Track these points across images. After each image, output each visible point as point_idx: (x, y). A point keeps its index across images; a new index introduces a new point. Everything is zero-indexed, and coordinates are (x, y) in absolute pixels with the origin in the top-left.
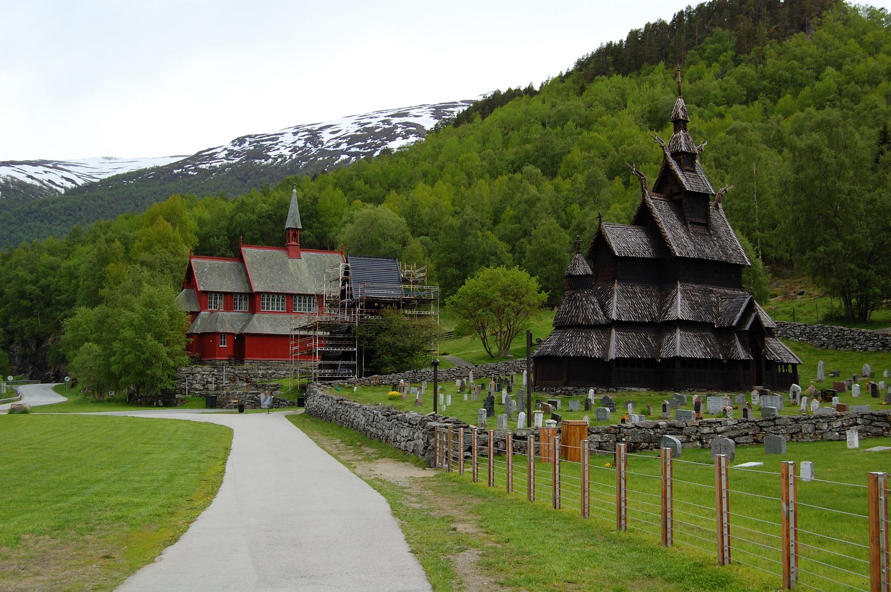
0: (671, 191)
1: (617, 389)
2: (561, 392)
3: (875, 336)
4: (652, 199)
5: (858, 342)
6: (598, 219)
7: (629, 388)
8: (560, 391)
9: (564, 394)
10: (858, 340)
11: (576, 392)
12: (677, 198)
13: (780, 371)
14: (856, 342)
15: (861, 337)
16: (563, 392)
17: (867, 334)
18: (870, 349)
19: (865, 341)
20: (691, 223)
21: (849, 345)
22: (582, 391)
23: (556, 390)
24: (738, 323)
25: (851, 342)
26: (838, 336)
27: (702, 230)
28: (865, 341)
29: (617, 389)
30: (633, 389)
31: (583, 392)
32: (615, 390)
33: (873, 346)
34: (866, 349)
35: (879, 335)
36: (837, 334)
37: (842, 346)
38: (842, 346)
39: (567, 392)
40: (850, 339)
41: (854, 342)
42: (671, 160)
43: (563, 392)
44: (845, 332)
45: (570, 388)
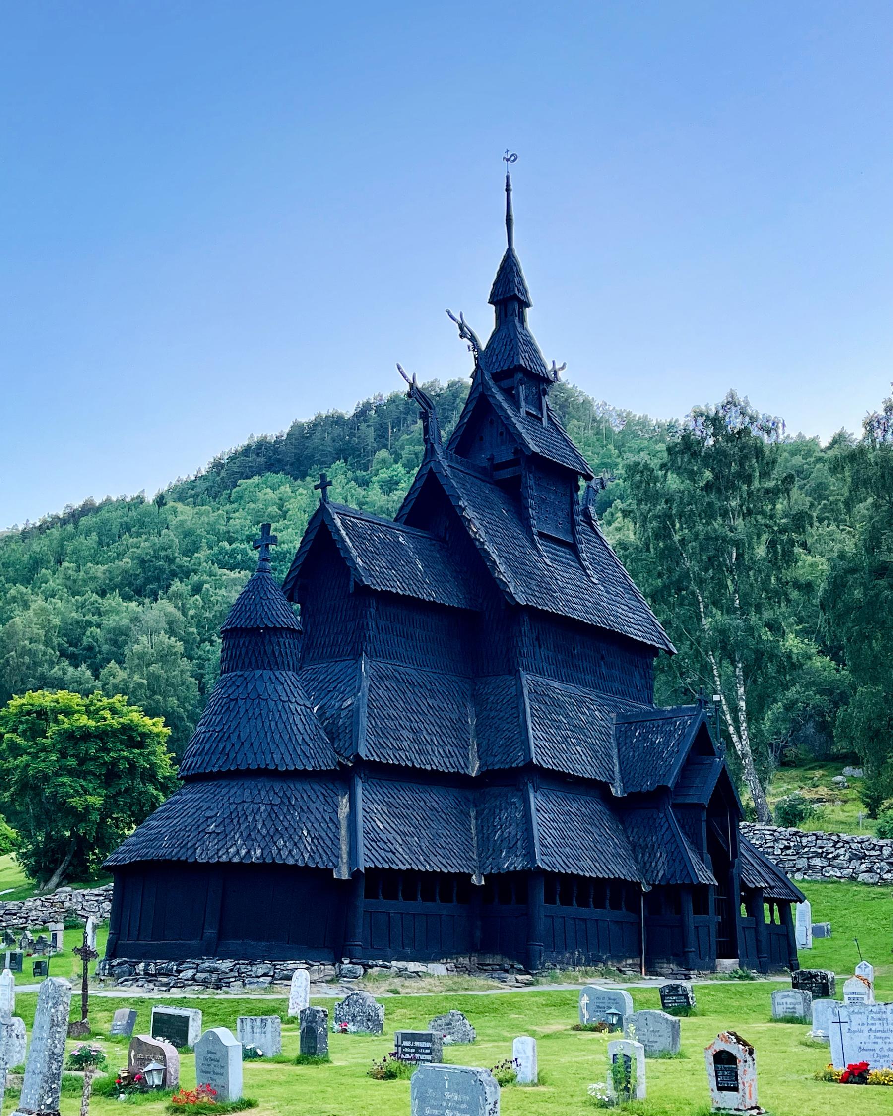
0: (491, 459)
1: (366, 967)
2: (193, 978)
3: (873, 849)
4: (449, 466)
5: (835, 862)
6: (320, 490)
7: (401, 964)
8: (190, 973)
9: (205, 983)
10: (834, 858)
11: (240, 976)
12: (506, 474)
13: (768, 920)
15: (842, 851)
16: (200, 976)
17: (854, 846)
18: (862, 877)
19: (850, 860)
20: (541, 535)
22: (261, 972)
23: (179, 972)
24: (677, 785)
25: (817, 862)
26: (788, 848)
27: (562, 552)
28: (850, 860)
29: (366, 967)
30: (413, 966)
31: (265, 975)
32: (360, 970)
33: (870, 870)
34: (853, 879)
35: (882, 847)
36: (785, 842)
37: (799, 870)
38: (799, 870)
39: (214, 976)
40: (819, 855)
41: (826, 863)
42: (491, 383)
43: (200, 976)
44: (804, 840)
45: (225, 965)
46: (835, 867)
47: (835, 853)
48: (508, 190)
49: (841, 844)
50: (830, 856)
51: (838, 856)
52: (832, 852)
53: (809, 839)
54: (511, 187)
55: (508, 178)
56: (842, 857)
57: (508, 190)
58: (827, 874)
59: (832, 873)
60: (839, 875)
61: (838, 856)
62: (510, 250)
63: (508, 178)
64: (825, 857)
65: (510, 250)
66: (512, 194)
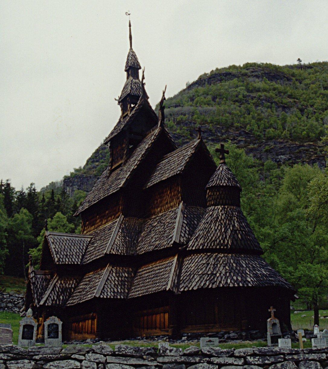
14: (16, 306)
15: (20, 301)
21: (8, 307)
25: (10, 305)
40: (10, 302)
46: (17, 307)
47: (18, 302)
48: (130, 26)
49: (20, 299)
50: (16, 303)
51: (19, 303)
52: (16, 302)
53: (7, 296)
54: (132, 25)
55: (130, 21)
56: (20, 304)
57: (130, 26)
58: (14, 310)
59: (16, 309)
60: (18, 310)
61: (19, 303)
62: (131, 48)
63: (130, 21)
64: (14, 303)
65: (131, 48)
66: (131, 27)
